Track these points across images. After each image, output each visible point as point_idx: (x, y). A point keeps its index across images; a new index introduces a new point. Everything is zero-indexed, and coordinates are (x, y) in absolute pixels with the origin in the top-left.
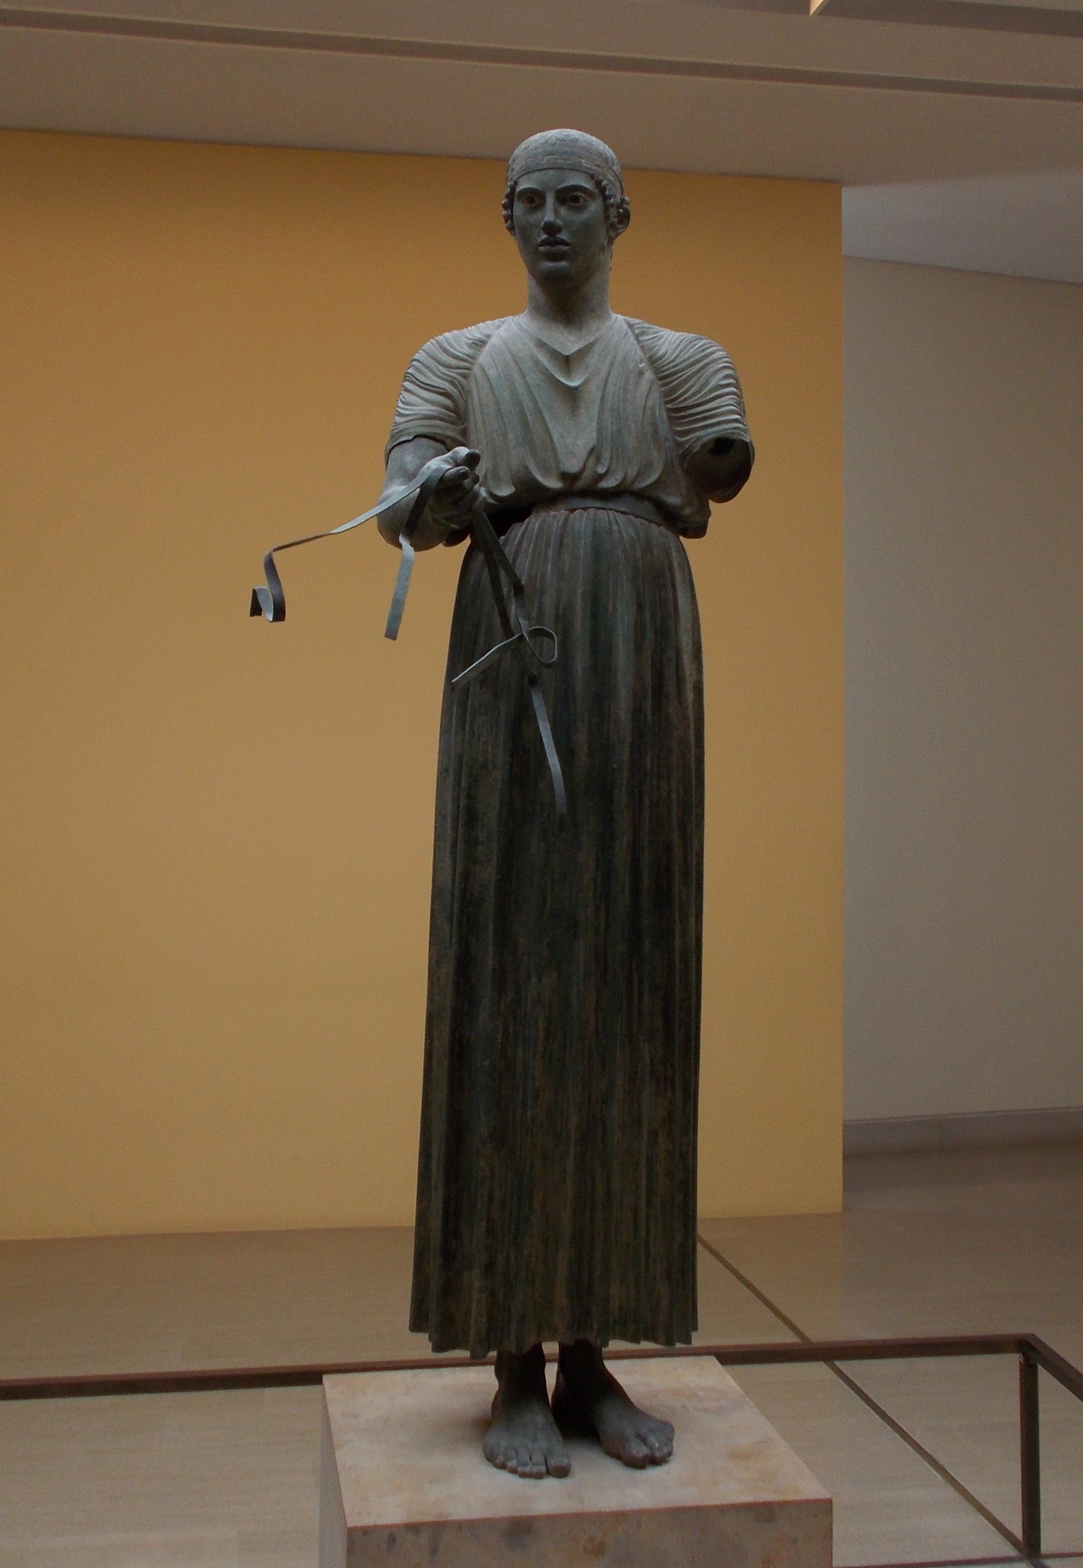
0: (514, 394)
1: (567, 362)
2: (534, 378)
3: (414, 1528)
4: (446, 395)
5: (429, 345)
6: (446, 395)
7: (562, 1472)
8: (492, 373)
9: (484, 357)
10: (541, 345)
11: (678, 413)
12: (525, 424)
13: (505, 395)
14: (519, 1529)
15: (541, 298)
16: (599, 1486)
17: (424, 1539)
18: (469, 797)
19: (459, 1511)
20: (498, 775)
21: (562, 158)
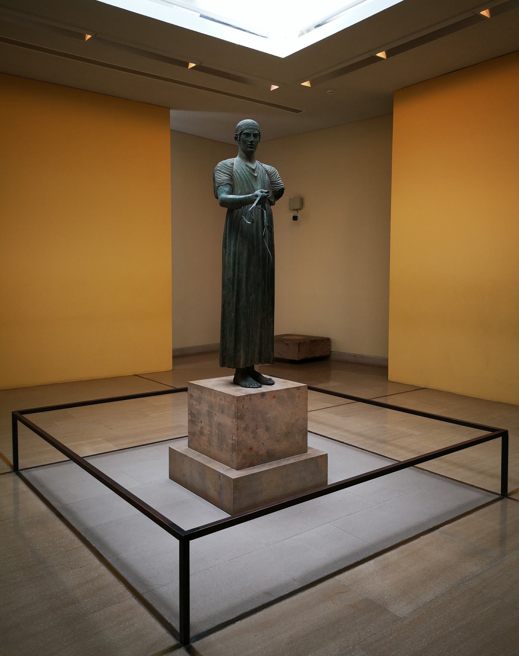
0: (244, 176)
1: (254, 170)
2: (247, 173)
3: (247, 396)
4: (230, 175)
5: (220, 163)
6: (230, 175)
7: (260, 387)
8: (239, 171)
9: (235, 167)
10: (247, 166)
11: (272, 183)
12: (247, 183)
13: (242, 176)
14: (263, 394)
15: (244, 155)
16: (265, 389)
17: (249, 397)
18: (239, 259)
19: (252, 393)
20: (245, 255)
21: (248, 126)
